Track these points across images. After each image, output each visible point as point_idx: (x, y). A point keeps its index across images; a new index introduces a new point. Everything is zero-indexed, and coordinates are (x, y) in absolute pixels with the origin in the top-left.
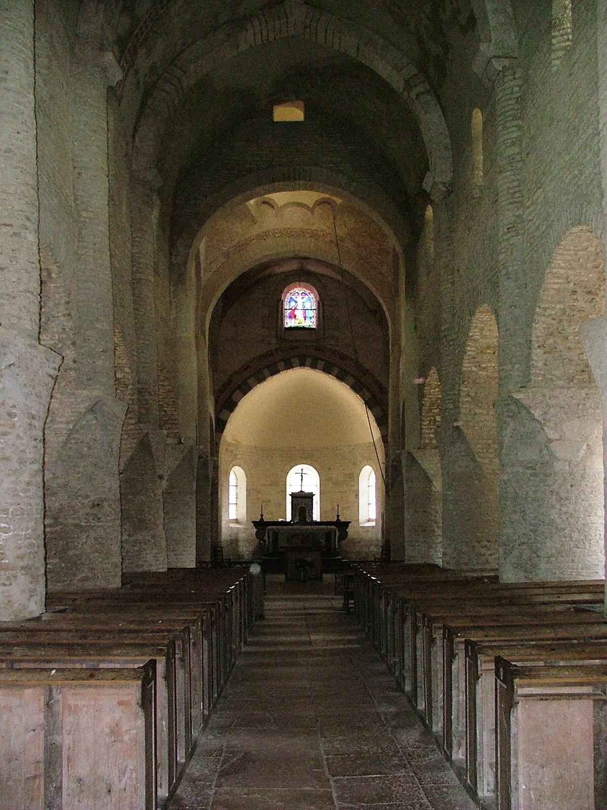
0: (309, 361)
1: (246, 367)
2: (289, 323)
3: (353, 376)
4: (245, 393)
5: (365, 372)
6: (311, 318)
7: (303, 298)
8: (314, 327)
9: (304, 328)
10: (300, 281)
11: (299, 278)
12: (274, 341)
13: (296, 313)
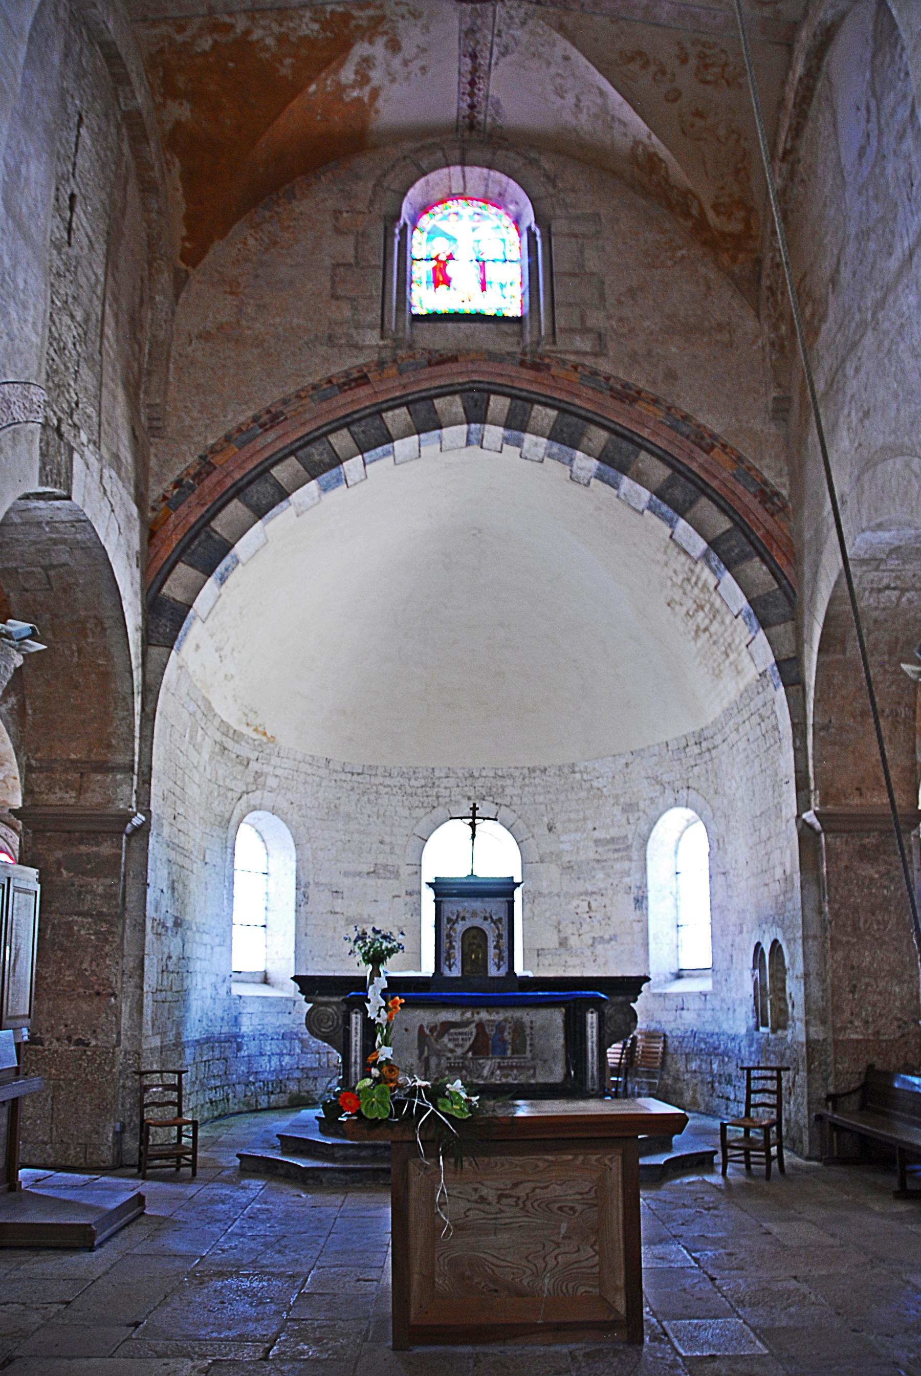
0: (499, 405)
1: (272, 419)
2: (425, 299)
3: (664, 457)
4: (260, 512)
5: (705, 441)
6: (502, 286)
7: (474, 230)
8: (514, 311)
9: (478, 318)
10: (463, 163)
11: (463, 152)
12: (372, 338)
13: (449, 271)
